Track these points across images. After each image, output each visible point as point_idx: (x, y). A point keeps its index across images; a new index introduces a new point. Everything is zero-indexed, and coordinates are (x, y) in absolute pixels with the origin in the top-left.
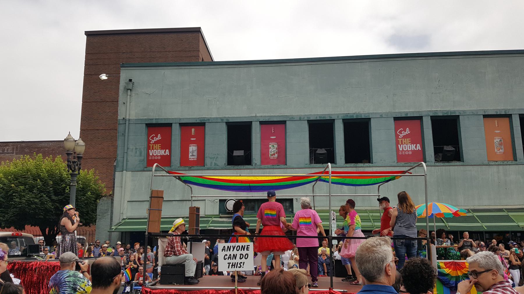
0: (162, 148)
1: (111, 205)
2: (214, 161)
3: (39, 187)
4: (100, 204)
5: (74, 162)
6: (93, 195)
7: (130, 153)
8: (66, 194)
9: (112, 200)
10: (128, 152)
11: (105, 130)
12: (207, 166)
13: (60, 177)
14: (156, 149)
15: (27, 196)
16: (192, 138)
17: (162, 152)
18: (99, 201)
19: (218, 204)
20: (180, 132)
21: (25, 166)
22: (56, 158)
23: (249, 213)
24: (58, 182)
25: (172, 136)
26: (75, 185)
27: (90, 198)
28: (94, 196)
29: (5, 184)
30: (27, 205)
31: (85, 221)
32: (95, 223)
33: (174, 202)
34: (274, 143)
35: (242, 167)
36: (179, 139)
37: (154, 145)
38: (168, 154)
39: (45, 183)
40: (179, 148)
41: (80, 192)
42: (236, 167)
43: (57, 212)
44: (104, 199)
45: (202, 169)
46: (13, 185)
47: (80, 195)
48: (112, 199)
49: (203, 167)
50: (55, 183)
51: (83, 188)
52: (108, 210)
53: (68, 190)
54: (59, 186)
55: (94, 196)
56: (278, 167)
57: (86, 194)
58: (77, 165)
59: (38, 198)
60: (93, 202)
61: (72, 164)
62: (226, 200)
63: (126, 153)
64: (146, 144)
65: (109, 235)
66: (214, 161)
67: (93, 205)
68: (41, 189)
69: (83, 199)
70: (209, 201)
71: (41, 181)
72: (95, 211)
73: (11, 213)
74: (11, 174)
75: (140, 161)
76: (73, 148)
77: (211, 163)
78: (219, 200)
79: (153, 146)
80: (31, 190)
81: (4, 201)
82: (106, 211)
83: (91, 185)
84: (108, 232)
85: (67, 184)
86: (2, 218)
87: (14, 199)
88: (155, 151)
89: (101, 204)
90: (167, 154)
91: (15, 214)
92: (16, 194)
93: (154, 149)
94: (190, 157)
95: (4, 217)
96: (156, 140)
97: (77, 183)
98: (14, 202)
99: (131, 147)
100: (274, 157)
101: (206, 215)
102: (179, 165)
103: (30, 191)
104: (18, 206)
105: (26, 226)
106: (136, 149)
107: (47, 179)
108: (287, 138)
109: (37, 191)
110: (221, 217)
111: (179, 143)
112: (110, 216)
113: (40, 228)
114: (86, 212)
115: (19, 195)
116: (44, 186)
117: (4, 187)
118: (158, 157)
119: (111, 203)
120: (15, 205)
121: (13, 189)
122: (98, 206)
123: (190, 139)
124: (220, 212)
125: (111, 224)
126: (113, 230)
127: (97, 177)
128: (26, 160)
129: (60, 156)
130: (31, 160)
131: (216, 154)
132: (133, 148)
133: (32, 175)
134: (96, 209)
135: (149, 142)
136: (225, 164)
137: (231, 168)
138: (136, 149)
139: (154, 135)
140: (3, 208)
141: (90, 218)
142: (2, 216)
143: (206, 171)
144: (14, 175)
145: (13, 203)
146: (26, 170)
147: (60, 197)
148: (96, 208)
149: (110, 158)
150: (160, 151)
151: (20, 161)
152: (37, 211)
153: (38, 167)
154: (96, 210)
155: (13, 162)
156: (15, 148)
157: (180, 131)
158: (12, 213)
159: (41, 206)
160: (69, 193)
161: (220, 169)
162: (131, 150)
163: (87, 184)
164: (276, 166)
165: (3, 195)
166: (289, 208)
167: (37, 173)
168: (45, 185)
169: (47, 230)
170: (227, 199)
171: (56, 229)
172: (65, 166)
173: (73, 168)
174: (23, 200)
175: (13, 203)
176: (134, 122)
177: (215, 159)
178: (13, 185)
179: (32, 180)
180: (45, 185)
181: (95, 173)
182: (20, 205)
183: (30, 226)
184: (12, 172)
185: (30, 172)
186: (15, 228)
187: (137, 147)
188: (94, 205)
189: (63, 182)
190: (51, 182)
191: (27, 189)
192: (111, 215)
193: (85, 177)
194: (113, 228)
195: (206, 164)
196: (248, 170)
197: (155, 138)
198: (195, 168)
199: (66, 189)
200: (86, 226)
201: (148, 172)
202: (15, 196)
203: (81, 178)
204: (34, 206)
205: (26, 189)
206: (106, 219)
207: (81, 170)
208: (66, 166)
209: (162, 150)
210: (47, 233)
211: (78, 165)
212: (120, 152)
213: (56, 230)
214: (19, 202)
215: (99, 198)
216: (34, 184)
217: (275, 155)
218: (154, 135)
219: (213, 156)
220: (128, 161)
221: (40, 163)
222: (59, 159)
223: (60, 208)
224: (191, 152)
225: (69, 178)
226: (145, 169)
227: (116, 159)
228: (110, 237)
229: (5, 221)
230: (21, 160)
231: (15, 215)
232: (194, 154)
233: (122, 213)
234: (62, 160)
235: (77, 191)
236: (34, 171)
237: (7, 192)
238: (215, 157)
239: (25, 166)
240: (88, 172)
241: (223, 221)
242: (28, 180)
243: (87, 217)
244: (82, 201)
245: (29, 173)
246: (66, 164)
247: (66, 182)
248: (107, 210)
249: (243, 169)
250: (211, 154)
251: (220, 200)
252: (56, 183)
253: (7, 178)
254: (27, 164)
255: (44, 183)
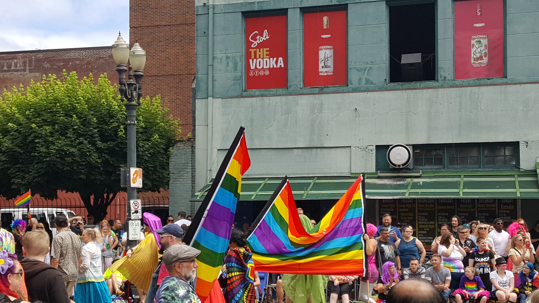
0: (271, 56)
1: (192, 156)
2: (365, 76)
3: (75, 127)
4: (174, 154)
5: (130, 85)
6: (163, 139)
7: (217, 65)
8: (119, 139)
9: (193, 147)
10: (215, 65)
11: (170, 25)
12: (352, 84)
13: (107, 109)
14: (262, 57)
15: (58, 143)
16: (323, 35)
17: (272, 63)
18: (173, 149)
19: (374, 154)
20: (301, 25)
21: (50, 93)
22: (99, 79)
23: (432, 169)
24: (105, 118)
25: (289, 32)
26: (134, 124)
27: (157, 144)
28: (163, 141)
29: (20, 124)
30: (57, 157)
31: (152, 184)
32: (167, 187)
33: (295, 150)
34: (480, 36)
35: (418, 84)
36: (301, 38)
37: (258, 50)
38: (283, 66)
39: (85, 120)
40: (302, 54)
41: (140, 135)
42: (407, 85)
43: (108, 170)
44: (180, 146)
45: (343, 90)
46: (34, 125)
47: (142, 140)
48: (192, 147)
49: (345, 88)
50: (101, 120)
51: (146, 128)
52: (187, 165)
53: (121, 131)
54: (108, 125)
55: (163, 141)
56: (489, 82)
57: (152, 138)
58: (135, 90)
59: (75, 146)
60: (162, 151)
61: (127, 87)
62: (389, 146)
63: (211, 66)
64: (244, 49)
65: (191, 206)
66: (365, 76)
67: (162, 157)
68: (79, 131)
69: (147, 146)
70: (357, 148)
71: (79, 118)
72: (165, 166)
73: (33, 172)
74: (29, 106)
75: (234, 81)
76: (127, 61)
77: (360, 79)
78: (375, 147)
79: (255, 52)
80: (62, 133)
81: (22, 152)
82: (183, 167)
83: (159, 124)
84: (190, 201)
85: (120, 122)
86: (20, 181)
87: (37, 149)
88: (260, 61)
89: (176, 154)
90: (281, 66)
91: (39, 172)
92: (41, 140)
93: (258, 57)
94: (321, 69)
95: (23, 178)
96: (260, 41)
97: (137, 119)
98: (38, 153)
99: (219, 55)
100: (480, 63)
101: (352, 174)
102: (302, 86)
103: (61, 134)
104: (44, 160)
105: (59, 192)
106: (228, 58)
107: (88, 114)
108: (507, 26)
109: (73, 135)
110: (379, 178)
111: (301, 44)
112: (191, 174)
113: (80, 193)
114: (152, 169)
115: (44, 142)
116: (84, 126)
117: (21, 128)
118: (264, 71)
119: (191, 152)
120: (41, 158)
121: (34, 132)
122: (171, 157)
123: (321, 36)
124: (378, 168)
125: (193, 187)
126: (198, 198)
127: (166, 109)
128: (52, 82)
129: (105, 74)
130: (59, 83)
131: (368, 63)
132: (222, 57)
133: (63, 108)
134: (168, 164)
135: (248, 45)
136: (385, 80)
137: (397, 87)
138: (228, 58)
139: (257, 32)
140: (21, 164)
141: (159, 177)
142: (20, 178)
143: (351, 94)
144: (35, 109)
145: (36, 154)
146: (53, 100)
147: (111, 144)
148: (168, 162)
149: (181, 75)
150: (268, 60)
151: (42, 84)
152: (75, 169)
153: (71, 94)
154: (169, 165)
155: (31, 86)
156: (28, 61)
157: (301, 21)
158: (36, 172)
159: (81, 159)
160: (124, 136)
161: (377, 89)
162: (219, 60)
163: (151, 121)
164: (486, 80)
165: (18, 142)
166: (511, 160)
167: (70, 104)
168: (85, 124)
169: (92, 197)
170: (391, 145)
171: (105, 195)
172: (114, 91)
173: (129, 95)
174: (52, 150)
175: (36, 154)
176: (222, 10)
177: (367, 71)
178: (34, 125)
179: (63, 116)
180: (85, 125)
181: (163, 102)
182: (47, 157)
183: (64, 191)
184: (30, 103)
185: (59, 103)
186: (41, 196)
187: (229, 55)
188: (165, 156)
189: (114, 119)
190: (95, 119)
191: (57, 131)
192: (192, 174)
193: (147, 109)
194: (198, 195)
195: (351, 82)
196: (430, 90)
197: (258, 37)
198: (331, 89)
199: (119, 130)
200: (153, 191)
201: (250, 99)
202: (37, 143)
203: (142, 112)
204: (69, 159)
205: (56, 132)
206: (184, 180)
207: (141, 98)
208: (116, 90)
209: (271, 59)
210: (92, 204)
211: (137, 90)
212: (200, 64)
213: (105, 197)
214: (45, 153)
215: (172, 145)
216: (67, 123)
217: (482, 59)
218: (257, 32)
219: (363, 67)
220: (216, 81)
221: (75, 87)
222: (103, 79)
223: (111, 163)
224: (322, 61)
225: (122, 111)
226: (244, 94)
227: (195, 78)
228: (193, 210)
229: (25, 185)
230: (43, 82)
231: (41, 174)
232: (327, 63)
233: (210, 170)
234: (109, 81)
235: (137, 132)
236: (66, 101)
237: (26, 137)
238: (367, 67)
239: (50, 93)
240: (152, 102)
241: (385, 184)
242: (58, 117)
243: (154, 176)
244: (145, 151)
245: (58, 104)
246: (115, 87)
247: (118, 119)
248: (185, 165)
249: (420, 89)
250: (360, 62)
251: (378, 147)
252: (102, 120)
253: (23, 114)
254: (53, 90)
255: (83, 121)
